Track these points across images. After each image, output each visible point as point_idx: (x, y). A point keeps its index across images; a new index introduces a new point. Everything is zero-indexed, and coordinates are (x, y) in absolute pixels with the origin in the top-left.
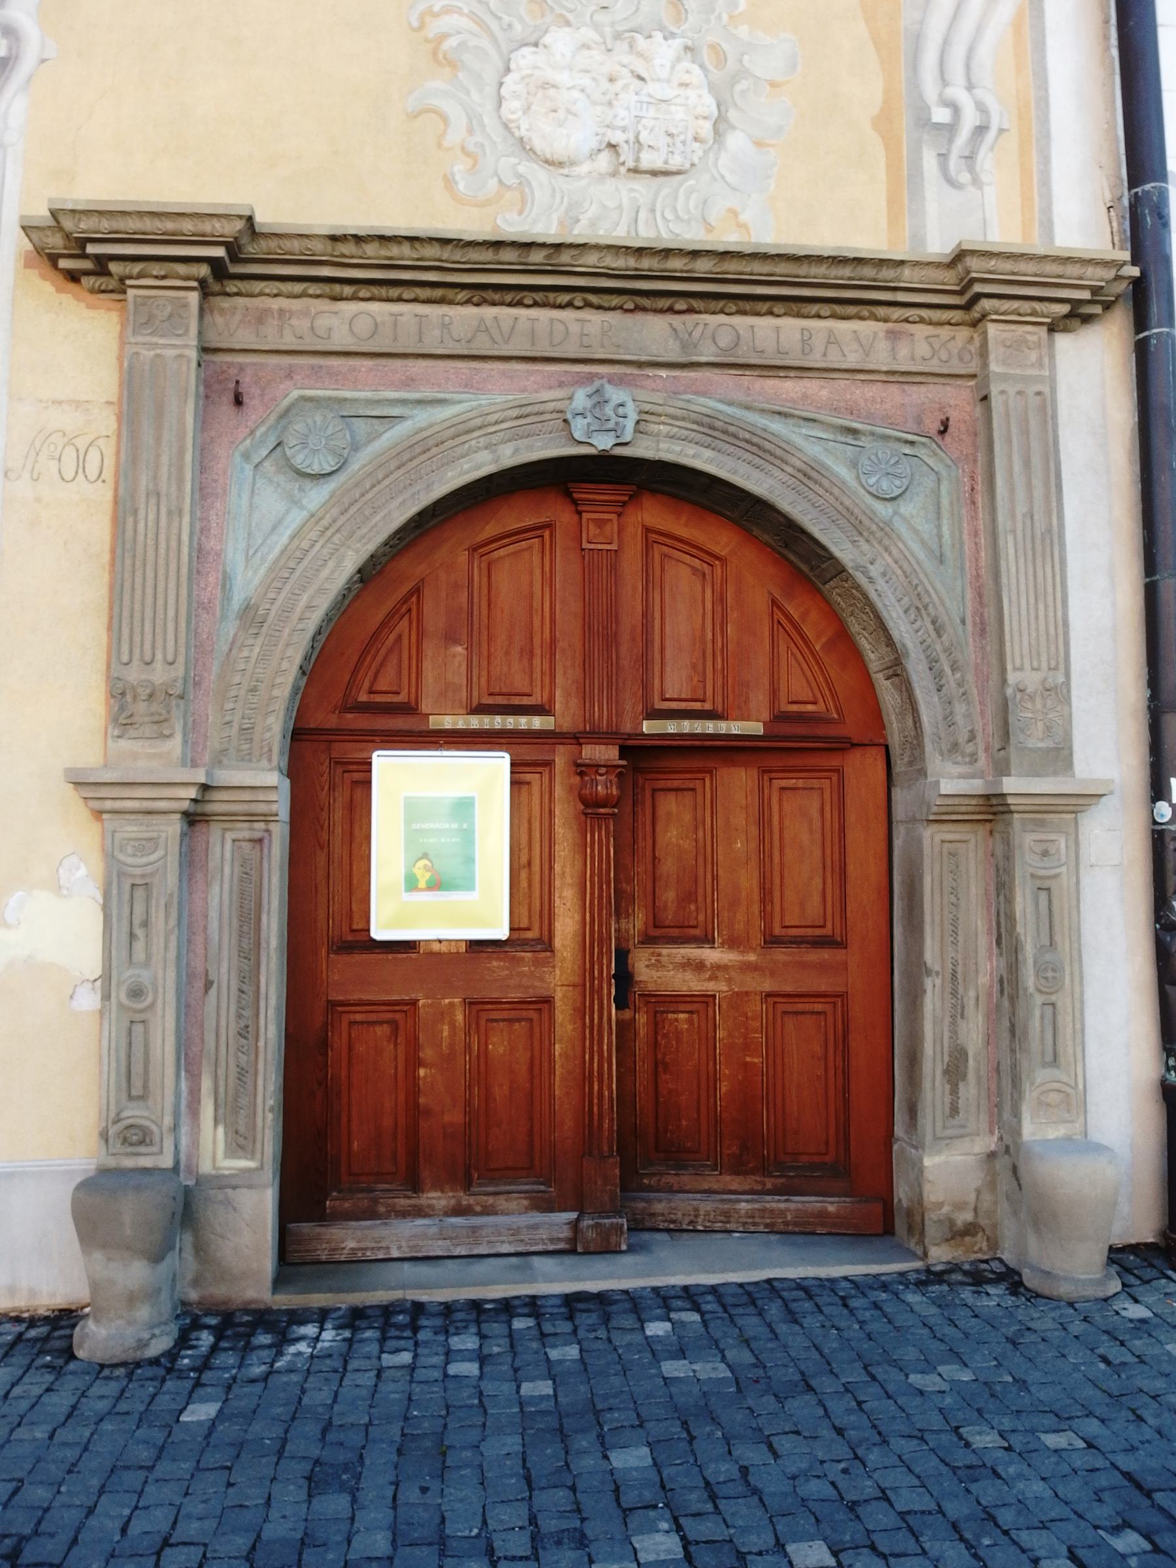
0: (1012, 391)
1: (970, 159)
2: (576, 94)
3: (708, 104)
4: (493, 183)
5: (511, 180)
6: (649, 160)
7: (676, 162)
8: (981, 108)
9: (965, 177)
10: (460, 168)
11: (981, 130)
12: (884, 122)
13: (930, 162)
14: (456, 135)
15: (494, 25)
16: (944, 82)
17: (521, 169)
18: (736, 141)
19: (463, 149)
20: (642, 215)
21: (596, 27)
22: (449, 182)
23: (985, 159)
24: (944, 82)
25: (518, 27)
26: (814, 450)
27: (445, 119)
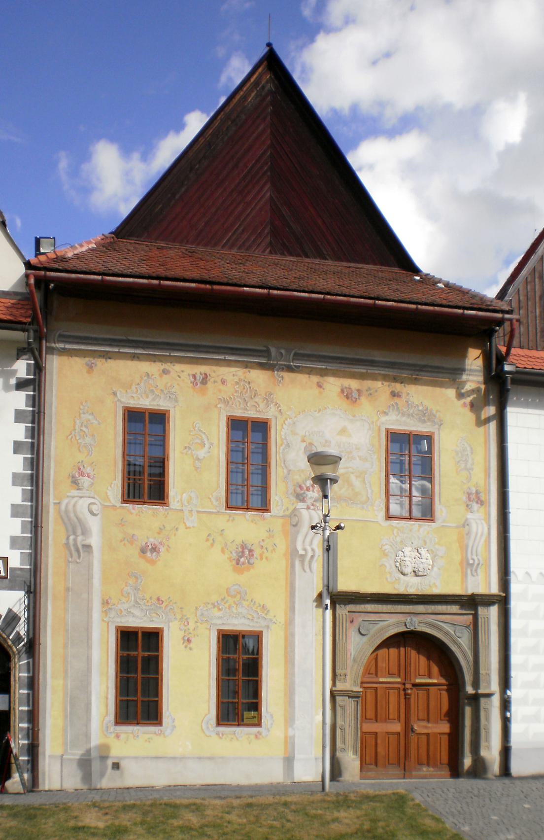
0: (482, 617)
1: (476, 570)
2: (409, 562)
3: (431, 563)
4: (394, 579)
5: (397, 579)
6: (420, 573)
7: (425, 574)
8: (478, 560)
9: (475, 574)
10: (388, 576)
11: (478, 564)
12: (461, 563)
13: (469, 571)
14: (387, 570)
15: (394, 547)
16: (472, 554)
17: (399, 576)
18: (435, 569)
19: (389, 572)
20: (419, 585)
21: (411, 546)
22: (387, 579)
23: (479, 571)
24: (472, 554)
25: (398, 548)
26: (447, 628)
27: (386, 566)
